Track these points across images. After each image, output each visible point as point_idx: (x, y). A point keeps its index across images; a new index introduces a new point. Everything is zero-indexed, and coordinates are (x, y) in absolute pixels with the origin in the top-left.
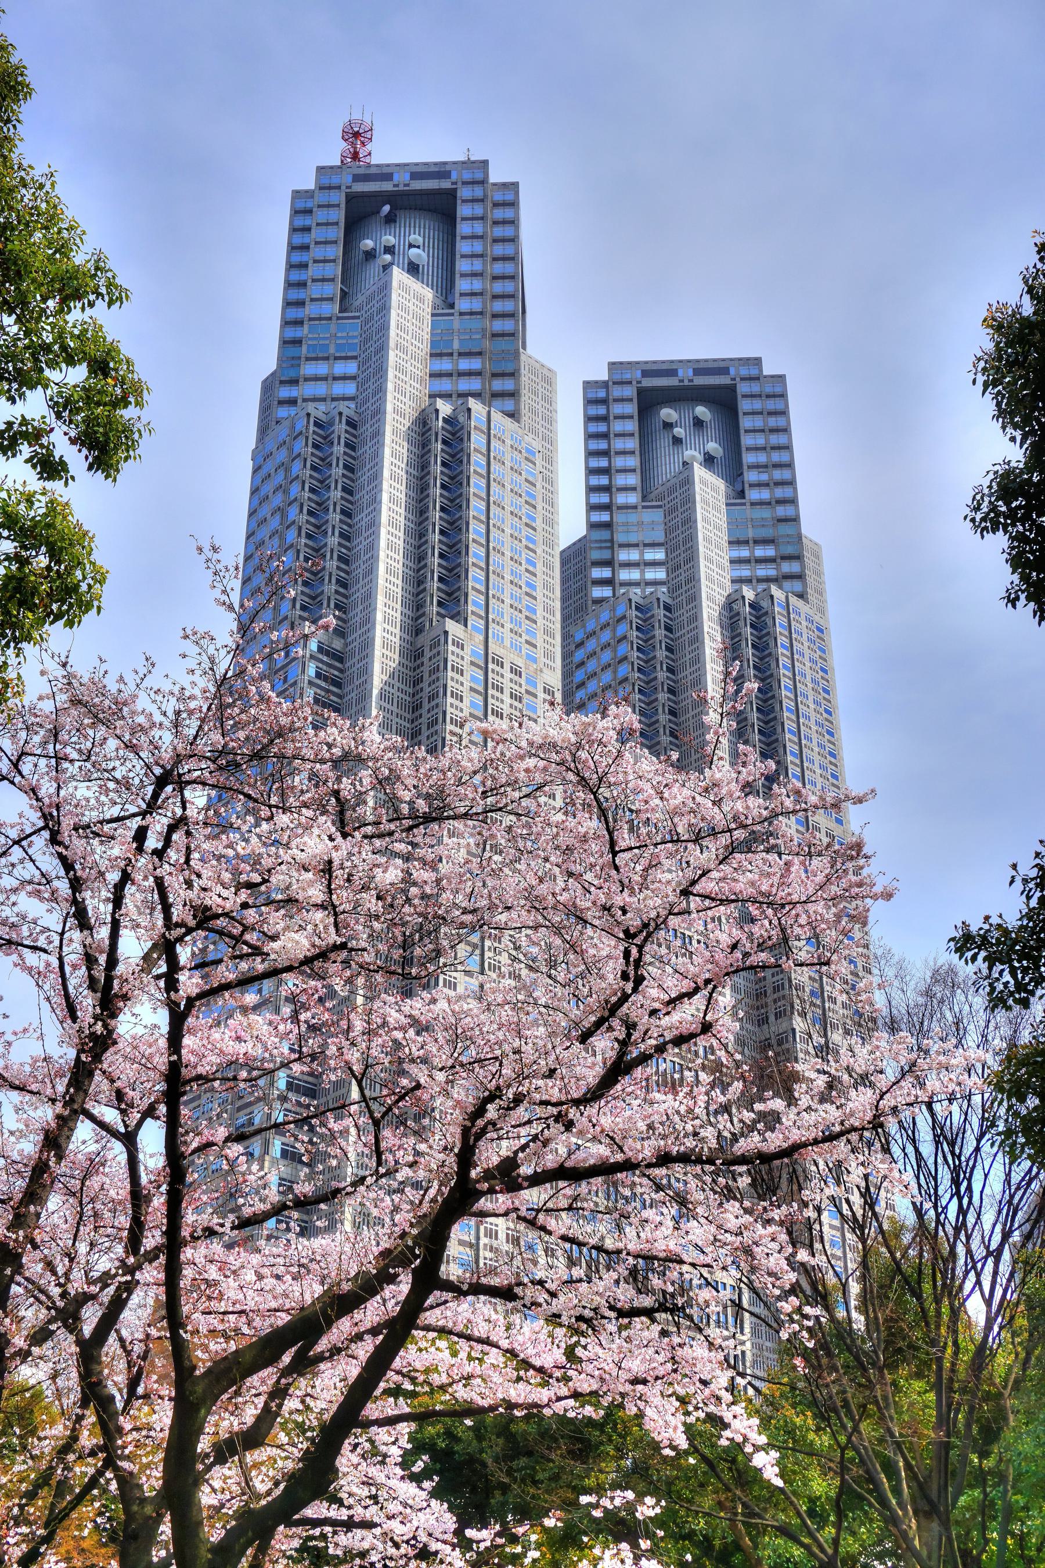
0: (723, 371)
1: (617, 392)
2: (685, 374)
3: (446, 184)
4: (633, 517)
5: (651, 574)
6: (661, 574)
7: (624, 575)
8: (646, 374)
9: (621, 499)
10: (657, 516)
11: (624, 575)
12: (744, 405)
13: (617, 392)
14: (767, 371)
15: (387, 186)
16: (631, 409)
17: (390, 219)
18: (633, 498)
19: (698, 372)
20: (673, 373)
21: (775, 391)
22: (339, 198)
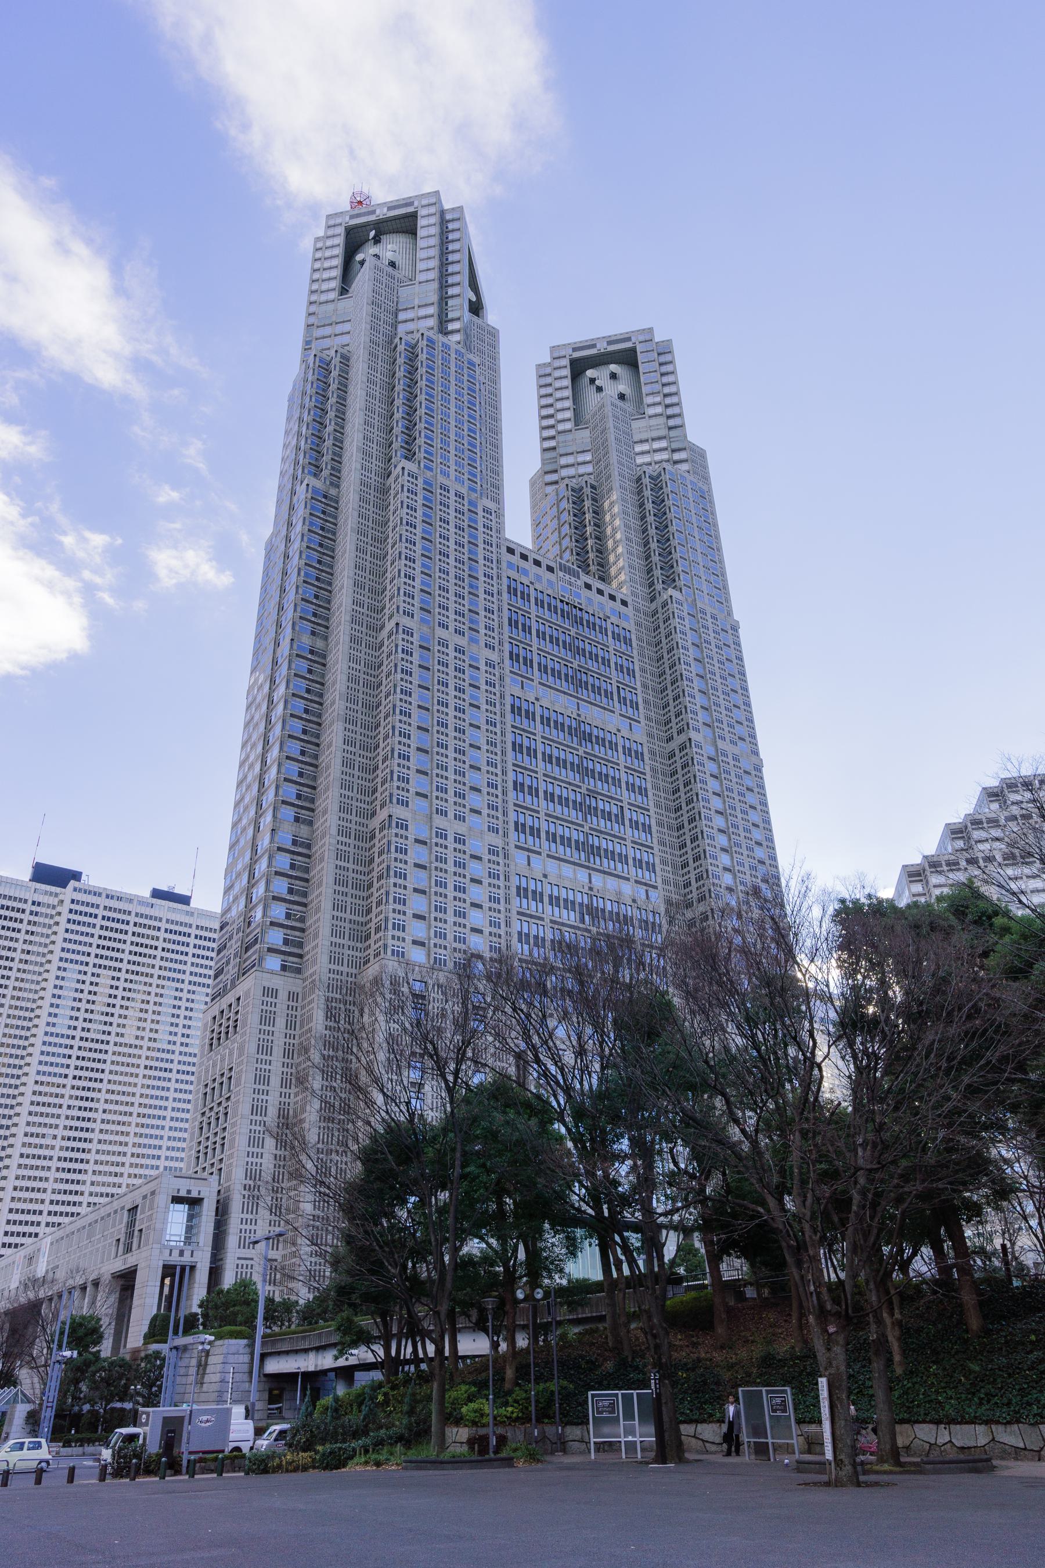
0: (629, 339)
1: (557, 363)
2: (602, 347)
3: (411, 209)
4: (569, 437)
5: (582, 470)
6: (589, 469)
7: (564, 472)
8: (574, 350)
9: (561, 427)
10: (586, 433)
11: (564, 472)
12: (641, 358)
13: (557, 363)
14: (658, 338)
15: (373, 218)
16: (567, 372)
17: (377, 240)
18: (568, 426)
19: (609, 343)
20: (594, 346)
21: (665, 351)
22: (341, 230)
